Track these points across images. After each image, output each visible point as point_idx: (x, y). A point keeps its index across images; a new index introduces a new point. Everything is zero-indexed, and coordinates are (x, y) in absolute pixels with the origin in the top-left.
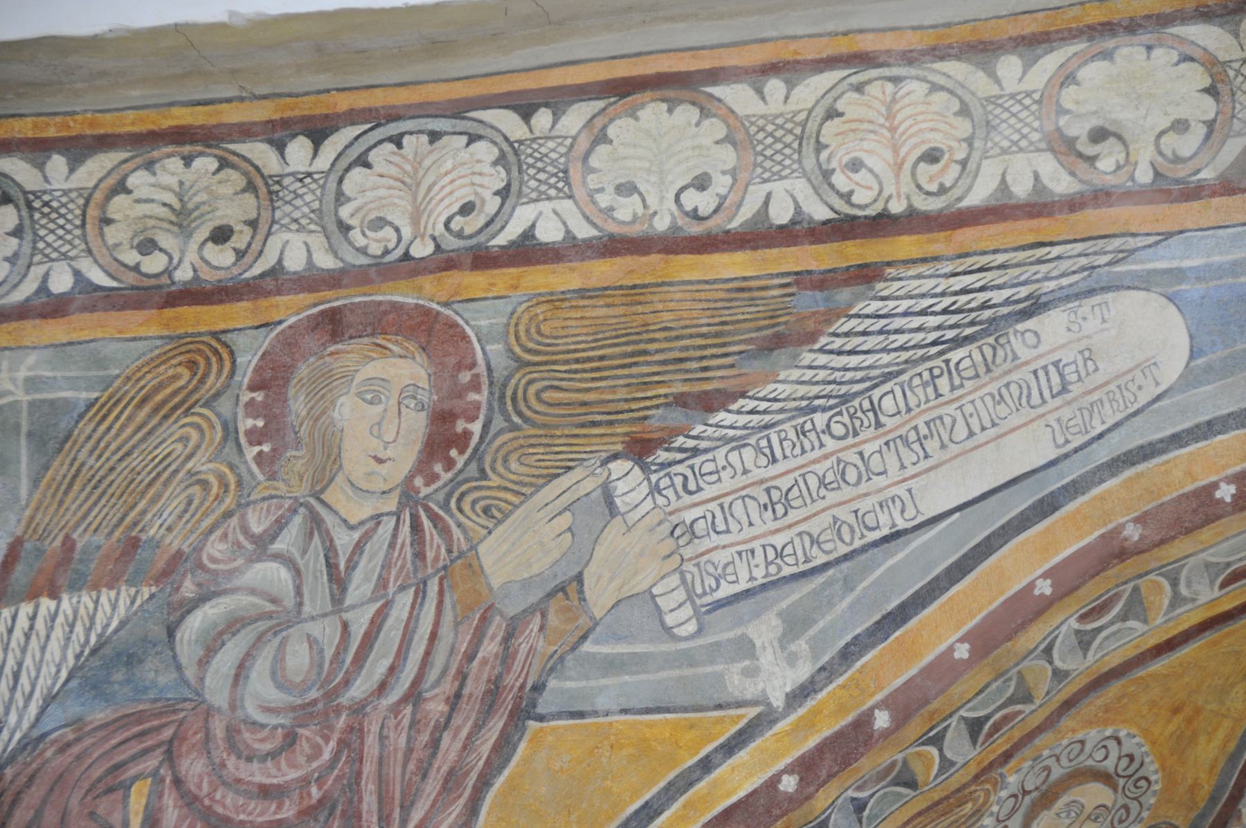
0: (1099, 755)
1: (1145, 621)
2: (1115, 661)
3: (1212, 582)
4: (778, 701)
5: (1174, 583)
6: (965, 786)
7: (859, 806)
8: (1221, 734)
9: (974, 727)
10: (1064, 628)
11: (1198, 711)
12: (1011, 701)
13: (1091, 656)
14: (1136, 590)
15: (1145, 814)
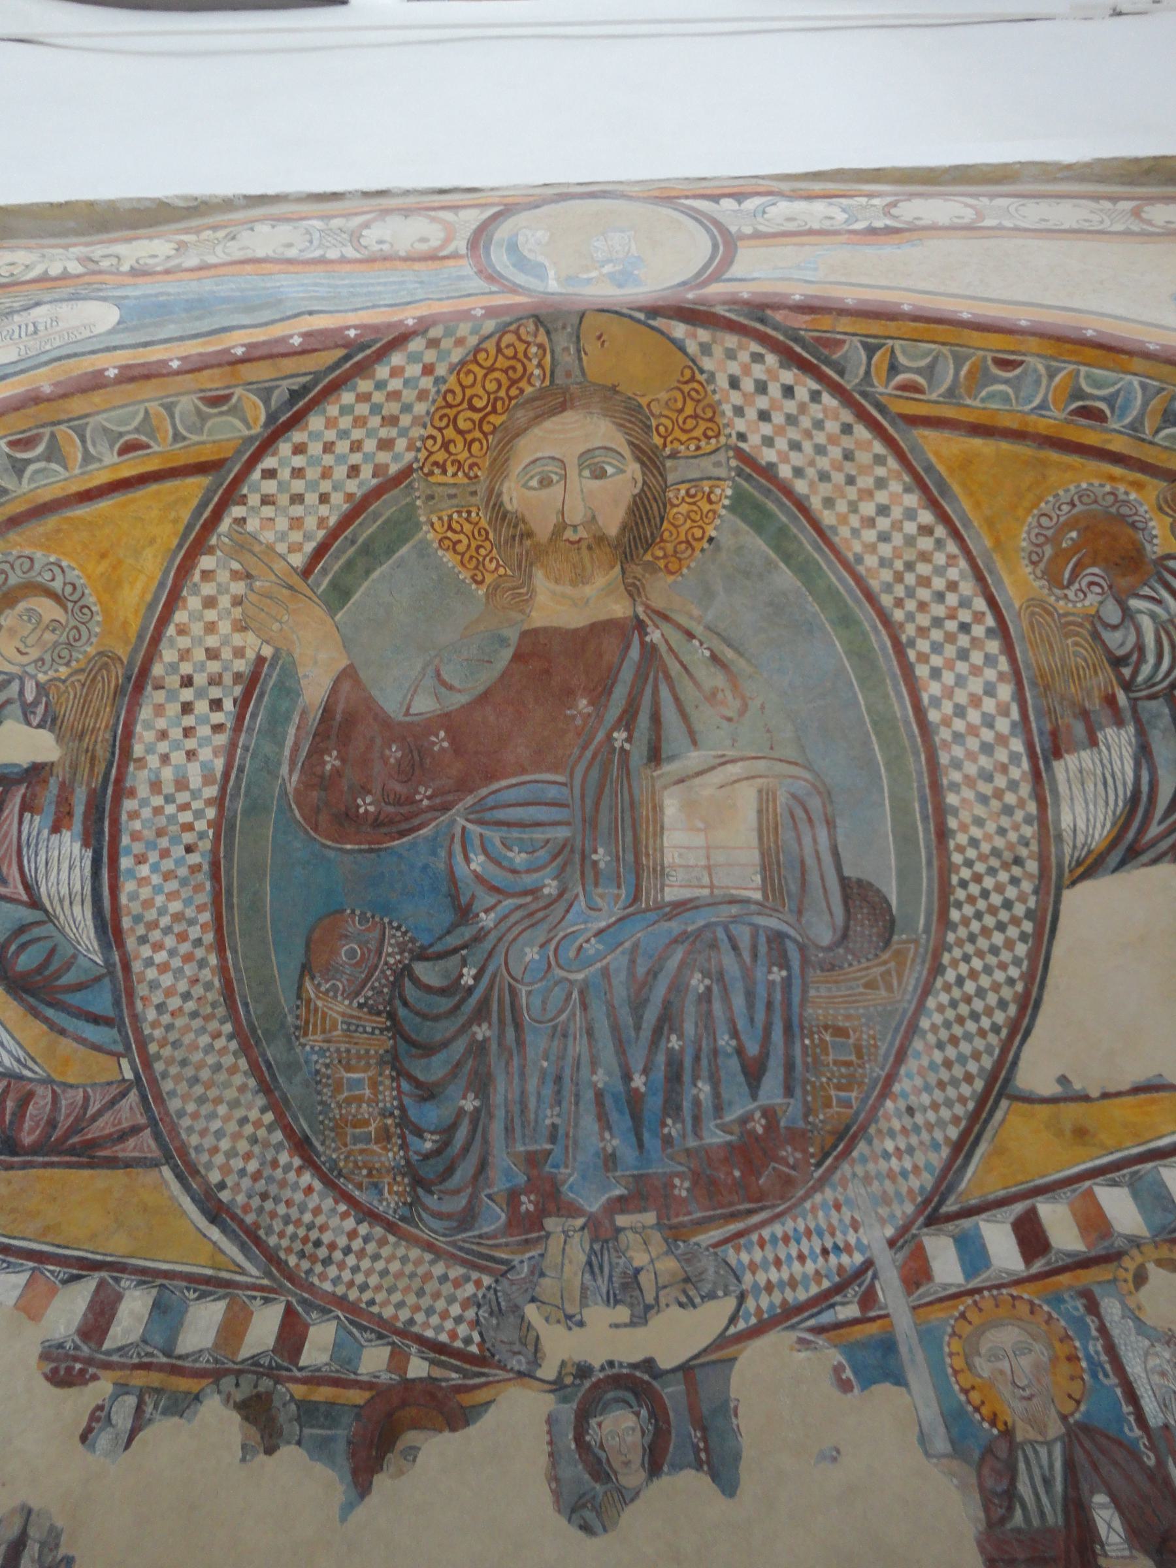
0: (48, 576)
1: (66, 468)
2: (46, 495)
3: (112, 447)
5: (83, 441)
8: (139, 586)
11: (120, 562)
13: (26, 486)
14: (53, 435)
15: (94, 640)
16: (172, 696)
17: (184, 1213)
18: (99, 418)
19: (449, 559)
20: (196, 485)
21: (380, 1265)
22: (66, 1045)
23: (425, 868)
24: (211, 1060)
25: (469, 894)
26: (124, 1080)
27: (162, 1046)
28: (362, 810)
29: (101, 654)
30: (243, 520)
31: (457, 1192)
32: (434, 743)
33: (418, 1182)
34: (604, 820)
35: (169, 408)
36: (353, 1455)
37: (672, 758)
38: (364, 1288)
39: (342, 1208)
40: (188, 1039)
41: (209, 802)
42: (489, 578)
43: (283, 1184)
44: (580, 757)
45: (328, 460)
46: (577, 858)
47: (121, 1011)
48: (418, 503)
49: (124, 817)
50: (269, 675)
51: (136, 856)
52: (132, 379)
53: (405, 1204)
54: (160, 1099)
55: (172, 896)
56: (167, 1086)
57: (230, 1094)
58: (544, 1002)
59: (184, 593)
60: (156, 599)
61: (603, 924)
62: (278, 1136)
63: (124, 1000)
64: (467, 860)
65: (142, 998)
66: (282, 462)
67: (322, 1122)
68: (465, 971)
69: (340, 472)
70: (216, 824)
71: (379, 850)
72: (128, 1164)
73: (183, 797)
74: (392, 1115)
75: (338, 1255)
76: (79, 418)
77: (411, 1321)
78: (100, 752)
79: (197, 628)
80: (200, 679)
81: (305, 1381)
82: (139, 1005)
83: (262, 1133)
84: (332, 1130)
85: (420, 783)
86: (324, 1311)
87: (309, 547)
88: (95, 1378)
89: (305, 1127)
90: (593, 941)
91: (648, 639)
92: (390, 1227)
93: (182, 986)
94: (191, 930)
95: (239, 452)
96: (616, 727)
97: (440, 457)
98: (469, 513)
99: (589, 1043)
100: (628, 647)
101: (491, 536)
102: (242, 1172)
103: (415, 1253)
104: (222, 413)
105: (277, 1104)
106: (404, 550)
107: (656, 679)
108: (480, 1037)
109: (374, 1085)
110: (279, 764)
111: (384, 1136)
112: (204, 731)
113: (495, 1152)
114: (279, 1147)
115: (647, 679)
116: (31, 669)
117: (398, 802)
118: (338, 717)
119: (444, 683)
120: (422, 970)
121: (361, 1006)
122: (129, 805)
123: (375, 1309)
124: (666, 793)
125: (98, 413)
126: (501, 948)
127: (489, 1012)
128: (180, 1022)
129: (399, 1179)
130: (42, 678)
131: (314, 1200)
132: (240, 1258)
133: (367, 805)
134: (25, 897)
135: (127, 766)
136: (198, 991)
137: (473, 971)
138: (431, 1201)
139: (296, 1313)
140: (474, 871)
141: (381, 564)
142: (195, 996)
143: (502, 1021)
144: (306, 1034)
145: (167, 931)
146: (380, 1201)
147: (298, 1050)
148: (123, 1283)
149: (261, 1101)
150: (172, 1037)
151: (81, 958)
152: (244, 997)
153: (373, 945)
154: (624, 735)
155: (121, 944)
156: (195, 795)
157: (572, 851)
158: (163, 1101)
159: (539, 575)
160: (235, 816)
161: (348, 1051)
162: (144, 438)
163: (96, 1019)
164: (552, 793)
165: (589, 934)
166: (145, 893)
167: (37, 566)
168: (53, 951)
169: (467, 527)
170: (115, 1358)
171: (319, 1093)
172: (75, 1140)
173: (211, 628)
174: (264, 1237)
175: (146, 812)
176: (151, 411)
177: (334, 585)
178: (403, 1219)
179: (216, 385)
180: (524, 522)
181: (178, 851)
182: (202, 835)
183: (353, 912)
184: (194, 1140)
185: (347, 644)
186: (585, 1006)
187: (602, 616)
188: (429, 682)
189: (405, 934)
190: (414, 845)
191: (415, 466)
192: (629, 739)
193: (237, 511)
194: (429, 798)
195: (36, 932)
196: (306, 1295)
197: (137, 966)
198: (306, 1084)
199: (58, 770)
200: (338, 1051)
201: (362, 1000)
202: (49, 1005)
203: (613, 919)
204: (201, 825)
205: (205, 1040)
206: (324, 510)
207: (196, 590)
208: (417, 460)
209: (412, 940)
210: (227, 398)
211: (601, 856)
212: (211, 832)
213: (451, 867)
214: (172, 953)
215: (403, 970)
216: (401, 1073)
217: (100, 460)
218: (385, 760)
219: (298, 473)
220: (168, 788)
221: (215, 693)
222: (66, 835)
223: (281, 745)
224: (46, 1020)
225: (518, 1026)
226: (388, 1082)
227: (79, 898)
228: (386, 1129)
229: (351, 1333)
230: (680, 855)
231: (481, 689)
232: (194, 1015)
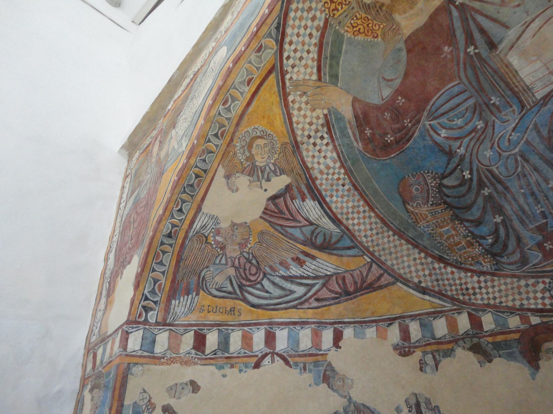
1: (239, 101)
2: (240, 112)
4: (184, 150)
5: (238, 90)
6: (226, 150)
7: (204, 160)
8: (278, 118)
9: (216, 135)
10: (220, 108)
11: (269, 116)
12: (220, 129)
13: (234, 113)
14: (230, 94)
15: (277, 142)
16: (308, 144)
17: (413, 294)
18: (236, 81)
19: (360, 38)
20: (272, 78)
21: (496, 289)
22: (345, 259)
23: (424, 147)
24: (392, 245)
25: (448, 146)
26: (368, 262)
27: (374, 247)
28: (389, 141)
29: (282, 145)
30: (291, 78)
31: (514, 253)
32: (399, 103)
33: (494, 255)
34: (486, 86)
35: (250, 62)
36: (524, 357)
37: (501, 41)
38: (495, 298)
39: (469, 274)
40: (380, 241)
41: (340, 168)
42: (379, 33)
43: (442, 274)
44: (459, 69)
45: (301, 39)
46: (484, 107)
47: (355, 242)
48: (337, 28)
49: (319, 187)
50: (331, 118)
51: (329, 196)
52: (236, 63)
53: (494, 264)
54: (382, 263)
55: (347, 202)
56: (383, 258)
57: (405, 252)
58: (507, 168)
59: (291, 112)
60: (285, 119)
61: (514, 125)
62: (430, 260)
63: (353, 239)
64: (439, 135)
65: (358, 236)
66: (289, 51)
67: (443, 249)
68: (464, 173)
69: (307, 39)
70: (346, 173)
71: (404, 150)
72: (386, 286)
73: (331, 171)
74: (468, 236)
75: (477, 291)
76: (232, 84)
77: (522, 304)
78: (300, 172)
79: (301, 119)
80: (312, 134)
81: (490, 336)
82: (359, 238)
83: (423, 261)
84: (448, 250)
85: (403, 119)
86: (484, 311)
87: (315, 70)
88: (414, 352)
89: (437, 252)
90: (513, 134)
91: (457, 3)
92: (493, 274)
93: (368, 227)
94: (360, 209)
95: (276, 59)
96: (467, 47)
97: (333, 6)
98: (356, 16)
99: (539, 174)
100: (451, 13)
101: (369, 17)
102: (425, 275)
103: (509, 280)
104: (263, 52)
105: (422, 249)
106: (344, 47)
107: (471, 16)
108: (487, 194)
109: (455, 229)
110: (352, 143)
111: (470, 244)
112: (324, 148)
113: (521, 232)
114: (432, 263)
115: (467, 19)
116: (268, 161)
117: (400, 130)
118: (361, 116)
119: (388, 80)
120: (445, 182)
121: (432, 205)
122: (318, 182)
123: (504, 304)
124: (508, 57)
125: (235, 79)
126: (474, 157)
127: (484, 183)
128: (374, 238)
129: (485, 257)
130: (272, 161)
131: (456, 275)
132: (441, 303)
133: (390, 138)
134: (308, 223)
135: (310, 171)
136: (374, 226)
137: (468, 172)
138: (504, 260)
139: (473, 314)
140: (444, 137)
141: (340, 58)
142: (374, 228)
143: (492, 184)
144: (418, 223)
145: (353, 213)
146: (483, 267)
147: (419, 229)
148: (406, 322)
149: (417, 251)
150: (375, 243)
151: (333, 233)
152: (390, 221)
153: (422, 183)
154: (473, 48)
155: (342, 223)
156: (334, 168)
157: (480, 106)
158: (385, 264)
159: (398, 17)
160: (350, 168)
161: (437, 222)
162: (250, 76)
163: (349, 248)
164: (456, 90)
165: (510, 132)
166: (339, 205)
167: (251, 132)
168: (325, 235)
169: (359, 22)
170: (417, 344)
171: (436, 240)
172: (365, 285)
173: (305, 116)
174: (446, 293)
175: (324, 182)
176: (247, 67)
177: (330, 76)
178: (496, 270)
179: (256, 45)
180: (378, 2)
181: (341, 188)
182: (344, 179)
183: (408, 176)
184: (402, 271)
185: (348, 91)
186: (527, 161)
187: (432, 10)
188: (383, 83)
189: (432, 173)
190: (415, 141)
191: (327, 17)
192: (476, 48)
193: (288, 77)
194: (410, 122)
195: (317, 231)
196: (473, 307)
197: (351, 227)
198: (428, 239)
199: (293, 184)
200: (433, 223)
201: (431, 203)
202: (334, 249)
203: (517, 121)
204: (342, 176)
205: (386, 240)
206: (311, 55)
207: (293, 108)
208: (326, 14)
209: (436, 173)
210: (261, 46)
211: (494, 100)
212: (346, 176)
213: (435, 141)
214: (359, 218)
215: (439, 185)
216: (462, 221)
217: (245, 92)
218: (386, 120)
219: (295, 51)
220: (325, 171)
221: (319, 134)
222: (307, 200)
223: (349, 137)
224: (335, 255)
225: (500, 182)
226: (459, 226)
227: (322, 216)
228: (469, 242)
229: (498, 315)
230: (533, 77)
231: (403, 73)
232: (377, 234)
